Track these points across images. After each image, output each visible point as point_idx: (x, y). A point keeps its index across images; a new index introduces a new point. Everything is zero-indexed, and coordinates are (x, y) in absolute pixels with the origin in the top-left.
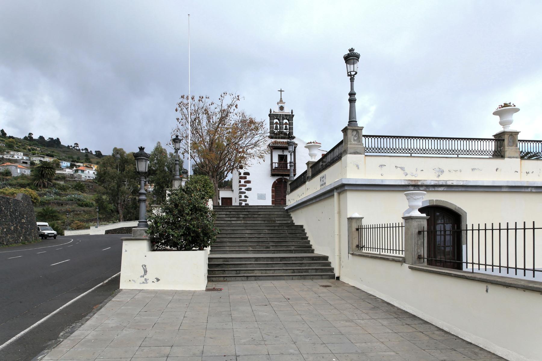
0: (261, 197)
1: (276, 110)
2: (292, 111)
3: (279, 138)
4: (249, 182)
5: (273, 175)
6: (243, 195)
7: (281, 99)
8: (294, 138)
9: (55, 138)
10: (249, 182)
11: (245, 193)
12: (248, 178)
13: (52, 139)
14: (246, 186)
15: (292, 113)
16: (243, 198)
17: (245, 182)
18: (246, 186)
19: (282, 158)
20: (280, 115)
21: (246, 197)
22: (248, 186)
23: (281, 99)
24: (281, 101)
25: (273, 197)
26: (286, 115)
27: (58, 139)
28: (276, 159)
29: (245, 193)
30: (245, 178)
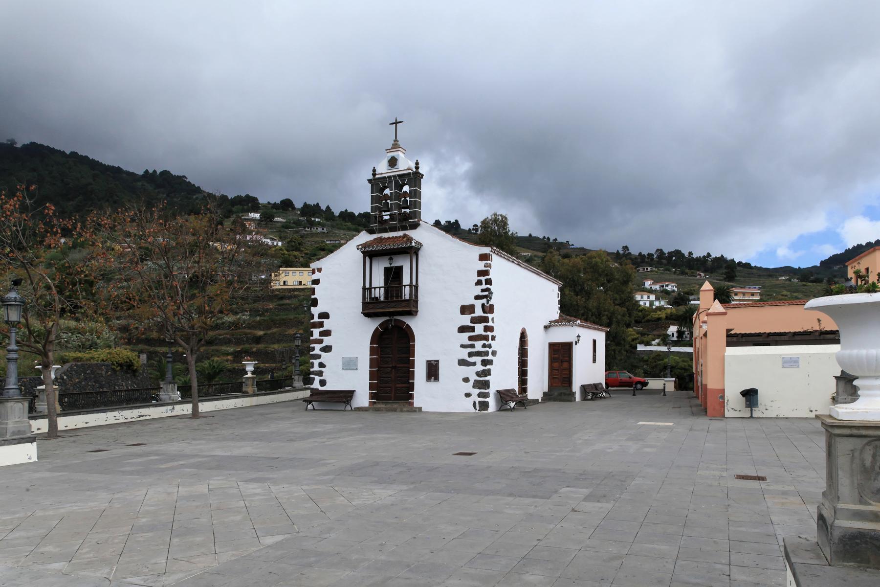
0: (350, 364)
1: (383, 169)
2: (417, 163)
3: (385, 231)
4: (327, 333)
5: (367, 314)
6: (316, 362)
7: (396, 140)
8: (415, 226)
9: (453, 221)
10: (327, 333)
11: (319, 357)
12: (327, 324)
13: (449, 222)
14: (321, 341)
15: (417, 168)
16: (316, 368)
17: (323, 334)
18: (321, 341)
19: (393, 276)
20: (389, 177)
21: (322, 365)
22: (327, 341)
23: (396, 140)
24: (396, 146)
25: (372, 363)
26: (400, 176)
27: (457, 221)
28: (379, 280)
29: (319, 357)
30: (321, 325)
